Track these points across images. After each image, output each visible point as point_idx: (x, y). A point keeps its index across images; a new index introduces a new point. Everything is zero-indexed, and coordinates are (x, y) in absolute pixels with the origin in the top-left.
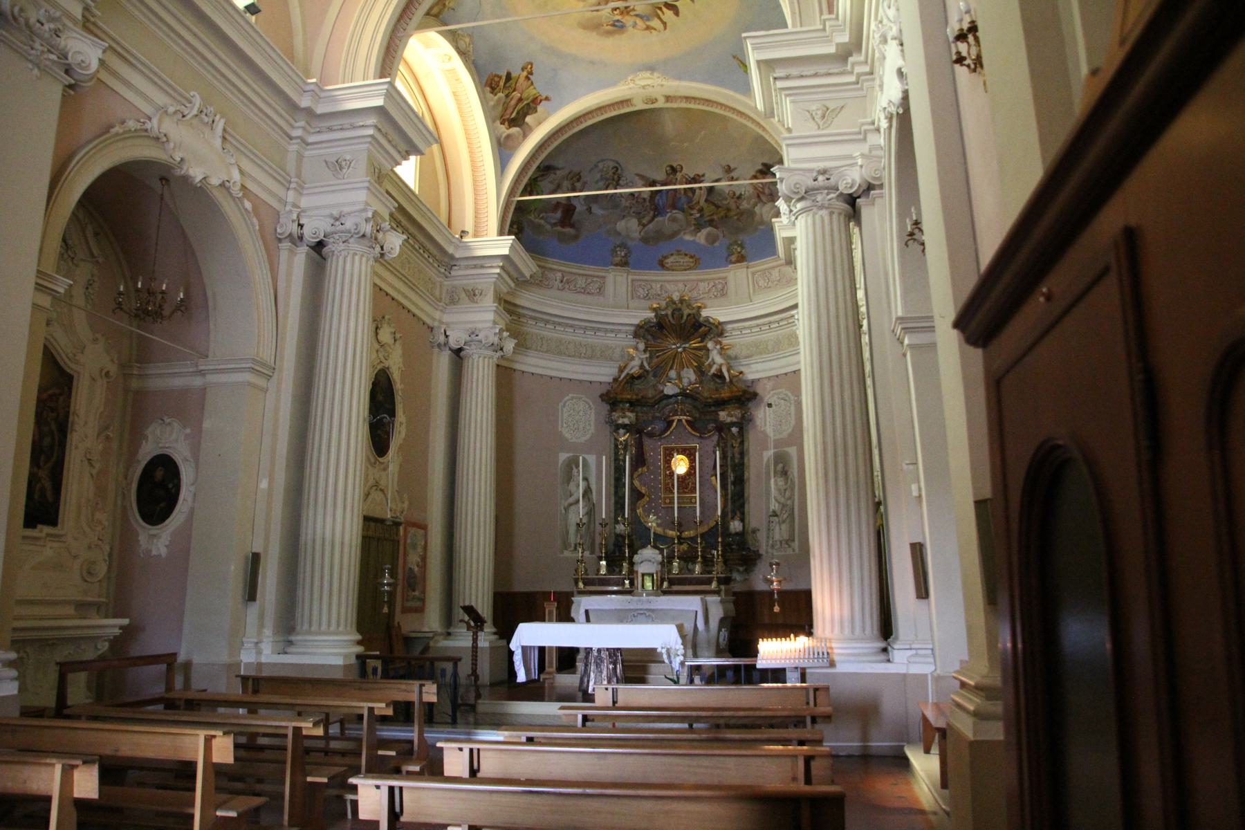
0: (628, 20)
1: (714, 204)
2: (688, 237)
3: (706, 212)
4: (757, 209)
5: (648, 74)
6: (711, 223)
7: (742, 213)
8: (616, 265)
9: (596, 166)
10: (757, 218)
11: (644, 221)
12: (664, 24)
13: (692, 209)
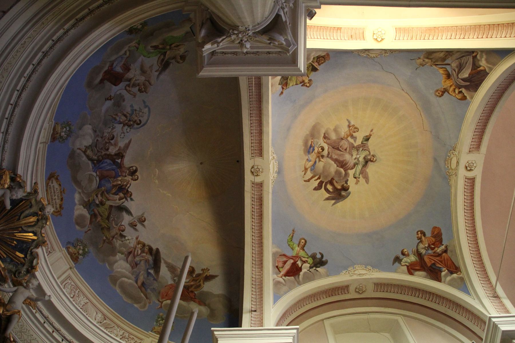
0: (313, 157)
1: (109, 214)
2: (77, 196)
3: (101, 209)
4: (119, 256)
5: (276, 169)
6: (94, 216)
7: (110, 243)
8: (54, 129)
9: (146, 106)
10: (111, 258)
11: (89, 152)
12: (309, 181)
13: (102, 195)
